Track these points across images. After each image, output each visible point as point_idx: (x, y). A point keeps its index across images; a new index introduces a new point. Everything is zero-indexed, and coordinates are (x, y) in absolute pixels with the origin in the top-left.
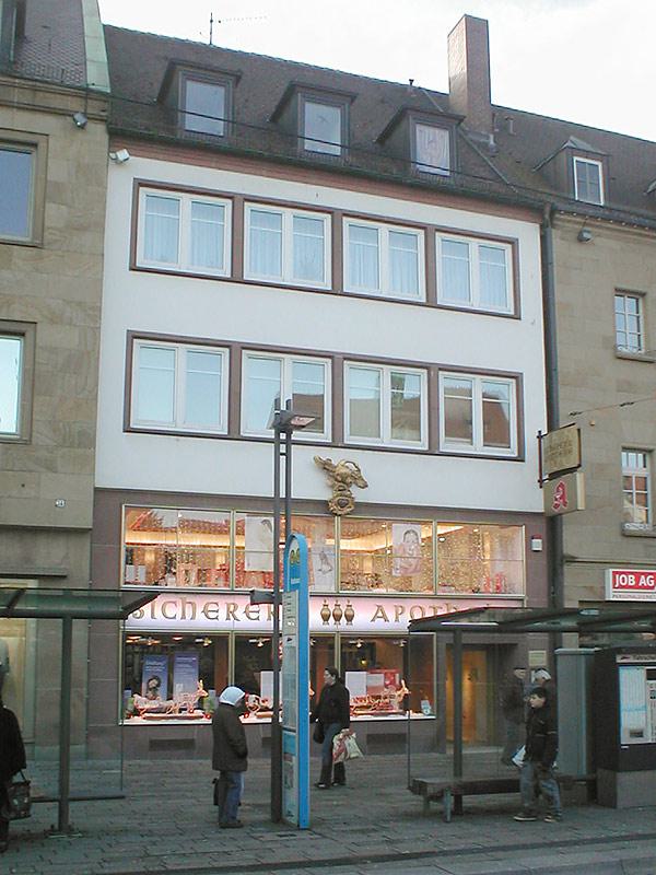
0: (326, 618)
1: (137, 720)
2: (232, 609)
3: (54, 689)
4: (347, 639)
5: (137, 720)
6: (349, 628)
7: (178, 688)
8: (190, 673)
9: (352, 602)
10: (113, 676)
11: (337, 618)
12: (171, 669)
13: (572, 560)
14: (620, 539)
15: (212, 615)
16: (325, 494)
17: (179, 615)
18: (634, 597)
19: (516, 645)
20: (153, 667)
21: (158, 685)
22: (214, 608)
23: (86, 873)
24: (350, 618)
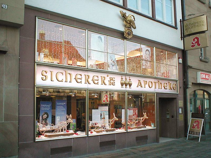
0: (122, 84)
1: (43, 138)
2: (103, 79)
3: (182, 96)
4: (129, 93)
5: (43, 138)
6: (130, 89)
7: (58, 119)
8: (63, 111)
9: (131, 78)
10: (30, 113)
11: (126, 85)
12: (53, 107)
13: (191, 67)
14: (199, 61)
15: (79, 81)
16: (122, 29)
17: (64, 80)
18: (205, 82)
19: (176, 98)
20: (45, 107)
21: (47, 117)
22: (96, 78)
23: (193, 157)
24: (130, 85)
